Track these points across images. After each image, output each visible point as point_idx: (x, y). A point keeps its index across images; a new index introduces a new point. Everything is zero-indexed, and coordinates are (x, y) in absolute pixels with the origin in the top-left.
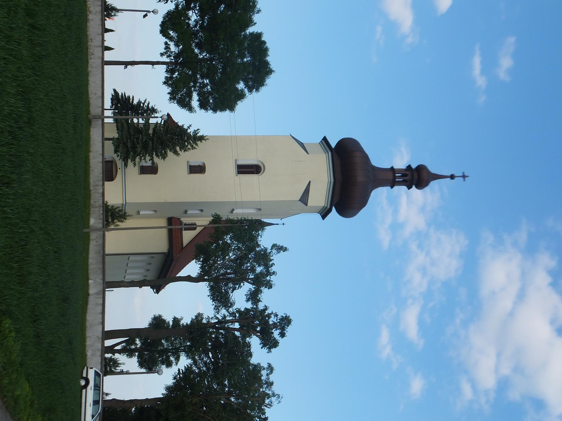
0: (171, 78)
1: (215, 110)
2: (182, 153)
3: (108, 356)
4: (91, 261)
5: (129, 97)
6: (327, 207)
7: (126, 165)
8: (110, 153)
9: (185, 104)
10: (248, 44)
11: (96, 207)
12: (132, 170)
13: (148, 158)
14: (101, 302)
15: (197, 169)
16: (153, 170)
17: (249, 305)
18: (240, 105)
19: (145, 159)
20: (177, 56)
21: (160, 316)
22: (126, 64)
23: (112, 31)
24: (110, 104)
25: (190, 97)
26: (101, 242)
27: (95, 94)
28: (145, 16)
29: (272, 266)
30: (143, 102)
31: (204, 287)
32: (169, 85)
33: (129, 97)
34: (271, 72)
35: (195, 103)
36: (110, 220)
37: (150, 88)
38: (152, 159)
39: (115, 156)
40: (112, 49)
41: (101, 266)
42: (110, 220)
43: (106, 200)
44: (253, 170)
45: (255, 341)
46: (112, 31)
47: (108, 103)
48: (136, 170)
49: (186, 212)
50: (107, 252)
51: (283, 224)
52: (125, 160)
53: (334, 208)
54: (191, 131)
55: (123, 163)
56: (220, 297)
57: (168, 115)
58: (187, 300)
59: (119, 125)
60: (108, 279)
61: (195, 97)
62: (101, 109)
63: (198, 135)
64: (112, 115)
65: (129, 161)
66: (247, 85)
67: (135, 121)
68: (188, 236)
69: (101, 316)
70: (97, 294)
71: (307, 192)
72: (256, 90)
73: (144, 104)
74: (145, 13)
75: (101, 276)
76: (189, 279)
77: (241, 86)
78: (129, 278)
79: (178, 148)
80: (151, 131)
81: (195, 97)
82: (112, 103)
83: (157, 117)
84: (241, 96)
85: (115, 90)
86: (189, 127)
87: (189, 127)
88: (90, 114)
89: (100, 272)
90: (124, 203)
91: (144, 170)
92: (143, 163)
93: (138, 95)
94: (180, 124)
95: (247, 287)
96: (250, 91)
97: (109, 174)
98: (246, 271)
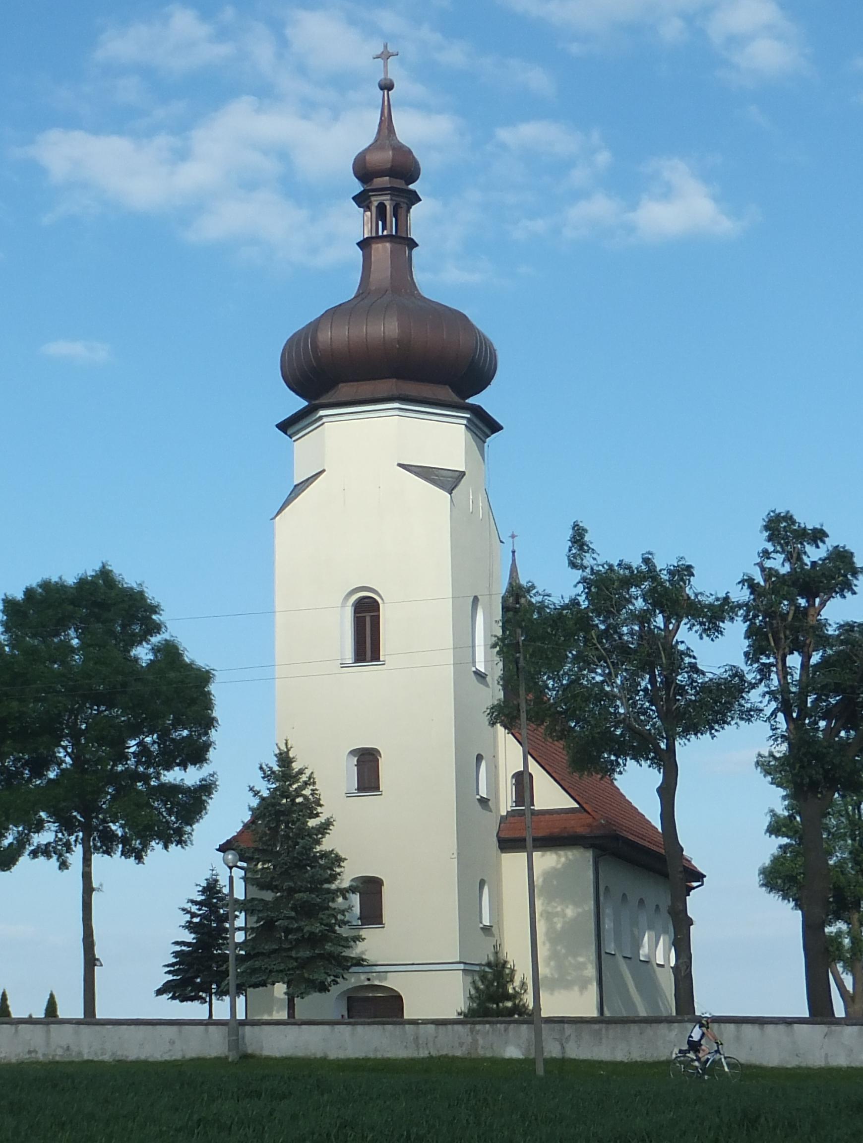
0: (125, 840)
1: (209, 723)
4: (620, 1056)
5: (176, 954)
6: (468, 419)
7: (359, 962)
8: (327, 1003)
10: (34, 636)
11: (475, 1041)
12: (373, 945)
14: (732, 1026)
15: (367, 768)
16: (371, 889)
18: (195, 654)
19: (343, 912)
20: (67, 825)
22: (91, 962)
24: (196, 1003)
27: (172, 1043)
29: (629, 567)
30: (188, 917)
31: (691, 751)
32: (145, 846)
33: (176, 954)
34: (105, 574)
35: (188, 776)
36: (509, 1004)
37: (151, 897)
38: (344, 892)
39: (335, 991)
40: (52, 997)
41: (634, 1028)
42: (509, 1004)
43: (454, 1016)
44: (368, 619)
47: (195, 1010)
49: (483, 802)
50: (594, 1013)
51: (513, 536)
53: (471, 400)
54: (265, 788)
55: (353, 969)
56: (717, 704)
57: (223, 849)
58: (724, 797)
59: (253, 980)
61: (173, 776)
62: (212, 1028)
63: (276, 768)
64: (227, 999)
65: (347, 953)
66: (142, 638)
67: (240, 937)
68: (549, 795)
69: (770, 1028)
72: (156, 613)
73: (193, 915)
75: (663, 1028)
76: (667, 792)
77: (143, 653)
79: (312, 823)
80: (268, 896)
81: (173, 776)
82: (192, 999)
83: (231, 879)
84: (170, 653)
85: (159, 992)
86: (256, 793)
87: (256, 793)
88: (227, 1058)
89: (650, 1030)
90: (462, 966)
91: (373, 914)
93: (172, 932)
94: (247, 817)
95: (687, 636)
96: (157, 628)
97: (384, 1007)
98: (647, 635)
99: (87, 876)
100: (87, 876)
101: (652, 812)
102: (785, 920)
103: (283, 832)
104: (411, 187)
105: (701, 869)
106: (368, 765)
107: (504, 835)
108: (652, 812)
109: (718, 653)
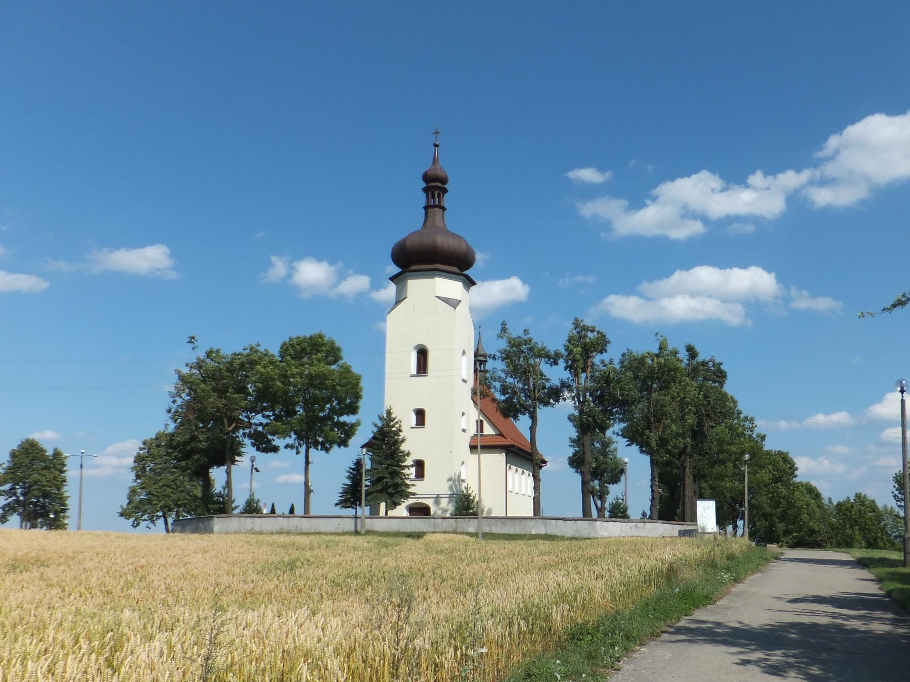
0: (323, 444)
2: (402, 435)
7: (414, 494)
8: (402, 510)
9: (348, 431)
11: (457, 526)
13: (406, 471)
16: (420, 465)
17: (562, 363)
18: (355, 370)
21: (570, 459)
22: (308, 491)
23: (273, 506)
25: (344, 424)
26: (493, 521)
28: (257, 470)
31: (542, 412)
32: (331, 447)
37: (333, 467)
38: (408, 467)
40: (293, 506)
41: (517, 521)
45: (597, 359)
46: (273, 506)
47: (350, 512)
49: (464, 431)
52: (407, 496)
56: (555, 394)
57: (363, 447)
60: (531, 515)
61: (344, 418)
65: (409, 490)
68: (488, 430)
70: (546, 525)
71: (446, 300)
76: (533, 429)
78: (531, 492)
81: (344, 418)
82: (349, 507)
84: (347, 370)
85: (337, 504)
86: (375, 425)
87: (375, 425)
89: (524, 522)
91: (420, 475)
92: (413, 477)
93: (342, 480)
95: (544, 367)
99: (307, 457)
100: (307, 457)
102: (576, 479)
103: (386, 442)
106: (420, 415)
108: (527, 435)
109: (556, 374)
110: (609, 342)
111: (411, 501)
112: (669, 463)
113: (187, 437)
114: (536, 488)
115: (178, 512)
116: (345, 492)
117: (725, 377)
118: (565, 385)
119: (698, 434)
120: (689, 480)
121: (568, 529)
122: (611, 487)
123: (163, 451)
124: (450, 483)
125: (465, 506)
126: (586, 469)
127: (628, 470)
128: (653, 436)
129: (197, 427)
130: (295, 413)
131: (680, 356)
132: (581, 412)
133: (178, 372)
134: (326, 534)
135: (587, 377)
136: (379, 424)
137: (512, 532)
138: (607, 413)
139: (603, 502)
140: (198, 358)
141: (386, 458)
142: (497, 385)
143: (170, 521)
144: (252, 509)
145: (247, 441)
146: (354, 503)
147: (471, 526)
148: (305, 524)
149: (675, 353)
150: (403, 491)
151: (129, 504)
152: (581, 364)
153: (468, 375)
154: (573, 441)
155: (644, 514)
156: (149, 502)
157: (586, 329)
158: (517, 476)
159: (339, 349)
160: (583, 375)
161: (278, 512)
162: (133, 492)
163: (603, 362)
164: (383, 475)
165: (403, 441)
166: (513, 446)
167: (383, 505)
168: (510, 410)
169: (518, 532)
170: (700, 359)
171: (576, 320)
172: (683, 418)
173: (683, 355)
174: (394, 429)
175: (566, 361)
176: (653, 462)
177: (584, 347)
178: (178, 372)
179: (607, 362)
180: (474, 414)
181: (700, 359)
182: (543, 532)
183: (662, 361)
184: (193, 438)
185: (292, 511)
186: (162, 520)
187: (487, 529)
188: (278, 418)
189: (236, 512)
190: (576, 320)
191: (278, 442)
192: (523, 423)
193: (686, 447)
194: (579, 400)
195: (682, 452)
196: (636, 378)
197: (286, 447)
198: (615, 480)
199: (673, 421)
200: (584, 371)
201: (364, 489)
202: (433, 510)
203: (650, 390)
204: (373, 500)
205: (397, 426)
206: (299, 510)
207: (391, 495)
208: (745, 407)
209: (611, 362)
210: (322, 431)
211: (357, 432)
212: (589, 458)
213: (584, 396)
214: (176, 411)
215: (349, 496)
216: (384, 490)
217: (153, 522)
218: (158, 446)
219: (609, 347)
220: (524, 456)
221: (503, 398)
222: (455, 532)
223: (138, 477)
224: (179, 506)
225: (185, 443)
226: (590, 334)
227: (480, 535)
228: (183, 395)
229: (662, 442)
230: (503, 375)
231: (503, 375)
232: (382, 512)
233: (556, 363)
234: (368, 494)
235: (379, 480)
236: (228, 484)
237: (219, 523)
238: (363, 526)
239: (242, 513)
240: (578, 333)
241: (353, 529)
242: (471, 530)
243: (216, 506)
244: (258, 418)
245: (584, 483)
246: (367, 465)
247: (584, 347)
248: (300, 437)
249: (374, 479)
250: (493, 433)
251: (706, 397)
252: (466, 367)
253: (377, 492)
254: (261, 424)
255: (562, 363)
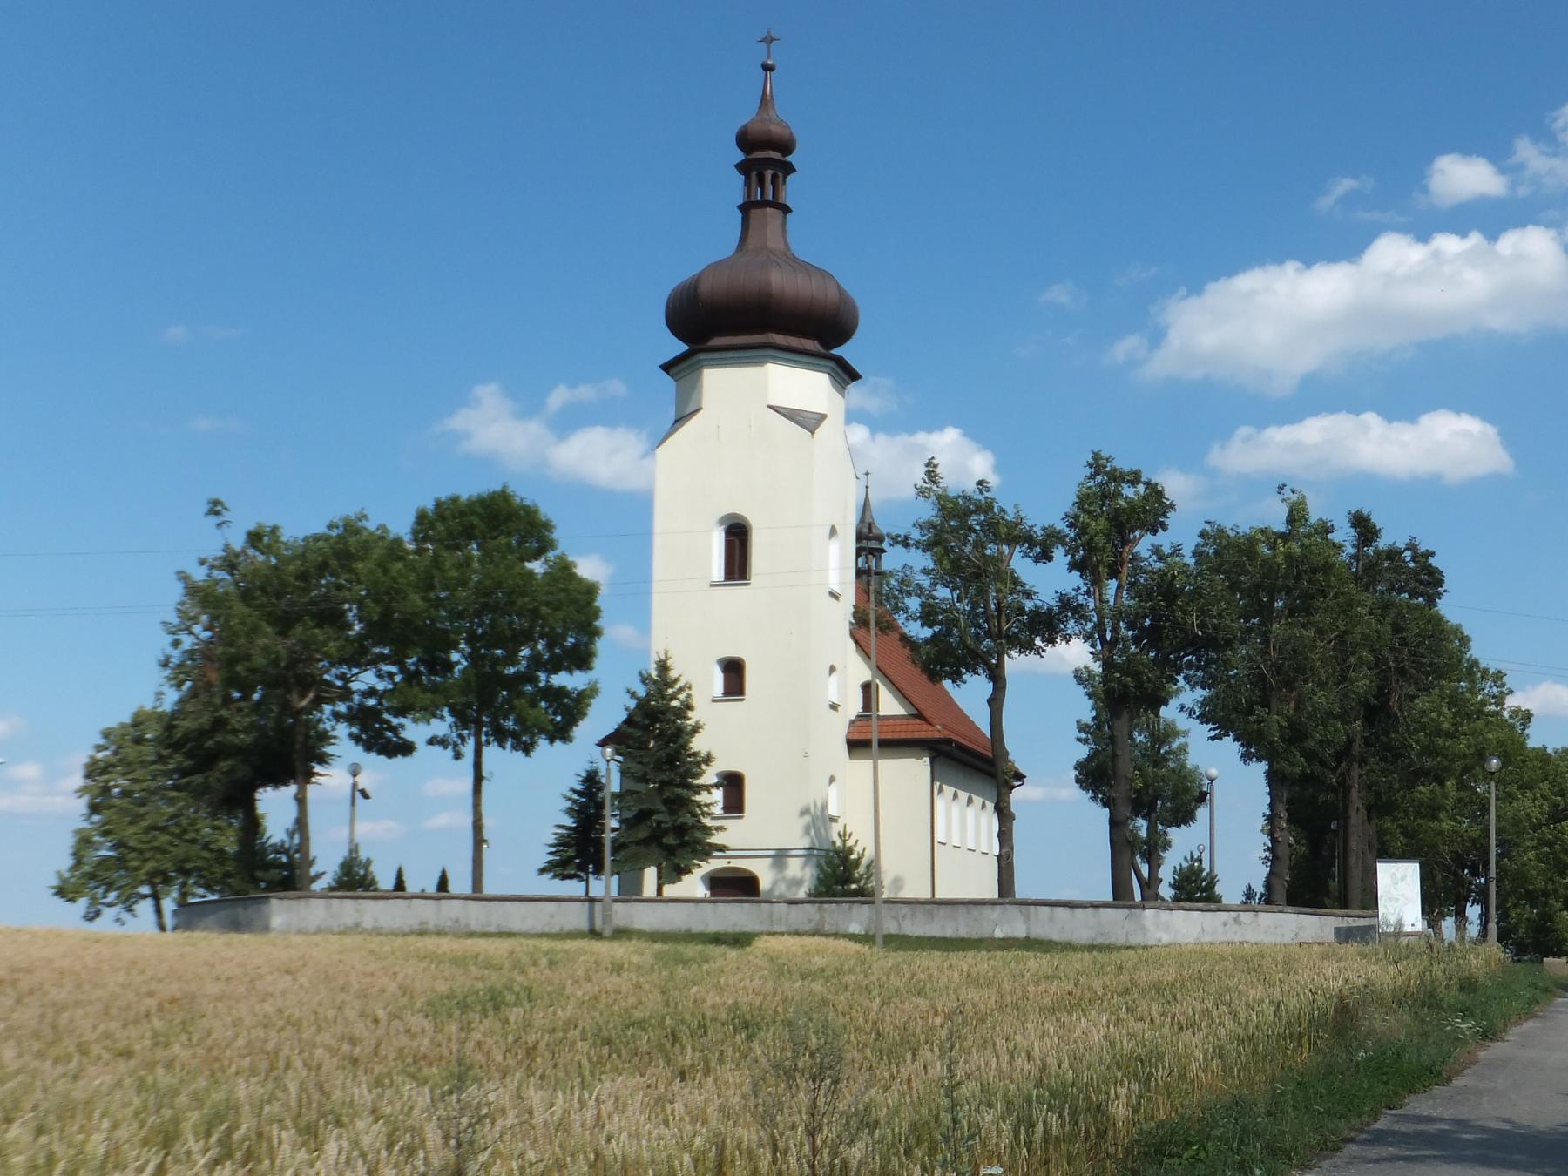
1: (596, 633)
2: (694, 717)
3: (1166, 891)
7: (722, 848)
8: (693, 885)
9: (570, 709)
11: (822, 918)
13: (703, 797)
16: (733, 784)
17: (1060, 556)
19: (707, 805)
21: (1079, 766)
25: (561, 692)
26: (905, 909)
27: (552, 916)
28: (365, 795)
30: (569, 804)
31: (1015, 663)
36: (854, 886)
37: (535, 788)
38: (707, 788)
42: (854, 886)
45: (1144, 545)
47: (574, 888)
48: (731, 824)
49: (834, 707)
50: (929, 896)
52: (707, 852)
53: (835, 352)
55: (716, 854)
56: (1046, 626)
57: (603, 743)
60: (993, 893)
61: (561, 679)
65: (712, 840)
66: (536, 555)
69: (1079, 911)
71: (792, 415)
73: (575, 802)
74: (358, 794)
75: (987, 910)
76: (995, 703)
77: (537, 567)
81: (561, 679)
83: (608, 770)
84: (564, 570)
85: (542, 871)
86: (633, 695)
87: (633, 695)
89: (975, 911)
91: (734, 804)
92: (718, 810)
95: (1021, 565)
101: (982, 722)
103: (656, 732)
104: (789, 158)
105: (1022, 771)
106: (734, 671)
107: (856, 737)
109: (1049, 581)
110: (1172, 506)
111: (715, 864)
112: (1306, 779)
113: (205, 720)
114: (1005, 836)
115: (184, 884)
116: (562, 843)
117: (1440, 583)
118: (1068, 606)
119: (1376, 711)
120: (1356, 817)
121: (1079, 927)
122: (1174, 833)
123: (149, 752)
124: (807, 818)
125: (840, 875)
126: (1120, 792)
127: (1219, 795)
128: (1275, 722)
129: (227, 700)
130: (450, 666)
131: (1335, 537)
132: (1108, 665)
133: (183, 577)
134: (526, 935)
135: (1119, 587)
136: (641, 692)
137: (949, 932)
138: (1168, 669)
139: (1154, 869)
140: (227, 548)
141: (658, 766)
142: (913, 603)
143: (168, 905)
144: (354, 880)
145: (342, 730)
146: (582, 867)
147: (856, 919)
148: (476, 914)
149: (1325, 529)
150: (699, 842)
151: (73, 869)
152: (1107, 558)
153: (842, 583)
154: (1083, 728)
155: (1249, 894)
156: (121, 862)
157: (1117, 477)
158: (956, 808)
159: (547, 526)
160: (1113, 583)
161: (412, 887)
162: (84, 842)
163: (1156, 551)
164: (652, 804)
165: (696, 729)
166: (948, 741)
167: (650, 874)
168: (946, 657)
169: (963, 932)
170: (1383, 543)
171: (1096, 456)
172: (1343, 678)
173: (1344, 535)
174: (675, 703)
175: (1071, 551)
176: (1273, 778)
177: (1113, 516)
178: (183, 577)
179: (1167, 550)
180: (859, 671)
181: (1383, 543)
182: (1020, 931)
183: (1296, 549)
184: (219, 724)
185: (443, 884)
186: (149, 903)
187: (891, 927)
188: (411, 677)
189: (317, 886)
190: (1096, 456)
191: (414, 731)
192: (970, 694)
193: (1350, 741)
194: (1103, 638)
195: (1343, 754)
196: (1234, 586)
197: (431, 742)
198: (1184, 816)
199: (1322, 685)
200: (1114, 573)
201: (608, 837)
202: (764, 884)
203: (1266, 613)
204: (629, 861)
205: (682, 696)
206: (460, 883)
207: (670, 852)
208: (1483, 651)
209: (1177, 551)
210: (512, 708)
211: (590, 711)
212: (1126, 767)
213: (1115, 629)
214: (180, 665)
215: (571, 852)
216: (655, 839)
217: (130, 910)
218: (139, 741)
219: (1172, 519)
220: (977, 764)
221: (927, 633)
222: (816, 933)
223: (94, 809)
224: (186, 873)
225: (203, 734)
226: (1128, 491)
227: (879, 940)
228: (197, 629)
229: (1295, 734)
230: (926, 582)
231: (926, 582)
232: (649, 889)
233: (1046, 556)
234: (617, 847)
235: (643, 816)
236: (301, 824)
237: (281, 912)
238: (607, 918)
239: (332, 889)
240: (1101, 484)
241: (584, 925)
242: (855, 928)
243: (274, 874)
244: (366, 679)
245: (1114, 824)
246: (613, 783)
247: (1113, 516)
248: (463, 719)
249: (629, 815)
250: (900, 711)
251: (1397, 629)
252: (837, 565)
253: (638, 843)
254: (371, 692)
255: (1060, 556)
